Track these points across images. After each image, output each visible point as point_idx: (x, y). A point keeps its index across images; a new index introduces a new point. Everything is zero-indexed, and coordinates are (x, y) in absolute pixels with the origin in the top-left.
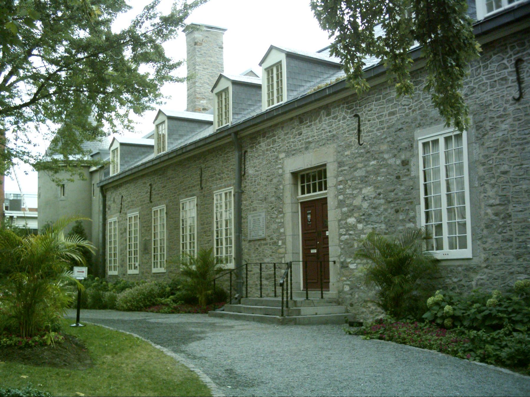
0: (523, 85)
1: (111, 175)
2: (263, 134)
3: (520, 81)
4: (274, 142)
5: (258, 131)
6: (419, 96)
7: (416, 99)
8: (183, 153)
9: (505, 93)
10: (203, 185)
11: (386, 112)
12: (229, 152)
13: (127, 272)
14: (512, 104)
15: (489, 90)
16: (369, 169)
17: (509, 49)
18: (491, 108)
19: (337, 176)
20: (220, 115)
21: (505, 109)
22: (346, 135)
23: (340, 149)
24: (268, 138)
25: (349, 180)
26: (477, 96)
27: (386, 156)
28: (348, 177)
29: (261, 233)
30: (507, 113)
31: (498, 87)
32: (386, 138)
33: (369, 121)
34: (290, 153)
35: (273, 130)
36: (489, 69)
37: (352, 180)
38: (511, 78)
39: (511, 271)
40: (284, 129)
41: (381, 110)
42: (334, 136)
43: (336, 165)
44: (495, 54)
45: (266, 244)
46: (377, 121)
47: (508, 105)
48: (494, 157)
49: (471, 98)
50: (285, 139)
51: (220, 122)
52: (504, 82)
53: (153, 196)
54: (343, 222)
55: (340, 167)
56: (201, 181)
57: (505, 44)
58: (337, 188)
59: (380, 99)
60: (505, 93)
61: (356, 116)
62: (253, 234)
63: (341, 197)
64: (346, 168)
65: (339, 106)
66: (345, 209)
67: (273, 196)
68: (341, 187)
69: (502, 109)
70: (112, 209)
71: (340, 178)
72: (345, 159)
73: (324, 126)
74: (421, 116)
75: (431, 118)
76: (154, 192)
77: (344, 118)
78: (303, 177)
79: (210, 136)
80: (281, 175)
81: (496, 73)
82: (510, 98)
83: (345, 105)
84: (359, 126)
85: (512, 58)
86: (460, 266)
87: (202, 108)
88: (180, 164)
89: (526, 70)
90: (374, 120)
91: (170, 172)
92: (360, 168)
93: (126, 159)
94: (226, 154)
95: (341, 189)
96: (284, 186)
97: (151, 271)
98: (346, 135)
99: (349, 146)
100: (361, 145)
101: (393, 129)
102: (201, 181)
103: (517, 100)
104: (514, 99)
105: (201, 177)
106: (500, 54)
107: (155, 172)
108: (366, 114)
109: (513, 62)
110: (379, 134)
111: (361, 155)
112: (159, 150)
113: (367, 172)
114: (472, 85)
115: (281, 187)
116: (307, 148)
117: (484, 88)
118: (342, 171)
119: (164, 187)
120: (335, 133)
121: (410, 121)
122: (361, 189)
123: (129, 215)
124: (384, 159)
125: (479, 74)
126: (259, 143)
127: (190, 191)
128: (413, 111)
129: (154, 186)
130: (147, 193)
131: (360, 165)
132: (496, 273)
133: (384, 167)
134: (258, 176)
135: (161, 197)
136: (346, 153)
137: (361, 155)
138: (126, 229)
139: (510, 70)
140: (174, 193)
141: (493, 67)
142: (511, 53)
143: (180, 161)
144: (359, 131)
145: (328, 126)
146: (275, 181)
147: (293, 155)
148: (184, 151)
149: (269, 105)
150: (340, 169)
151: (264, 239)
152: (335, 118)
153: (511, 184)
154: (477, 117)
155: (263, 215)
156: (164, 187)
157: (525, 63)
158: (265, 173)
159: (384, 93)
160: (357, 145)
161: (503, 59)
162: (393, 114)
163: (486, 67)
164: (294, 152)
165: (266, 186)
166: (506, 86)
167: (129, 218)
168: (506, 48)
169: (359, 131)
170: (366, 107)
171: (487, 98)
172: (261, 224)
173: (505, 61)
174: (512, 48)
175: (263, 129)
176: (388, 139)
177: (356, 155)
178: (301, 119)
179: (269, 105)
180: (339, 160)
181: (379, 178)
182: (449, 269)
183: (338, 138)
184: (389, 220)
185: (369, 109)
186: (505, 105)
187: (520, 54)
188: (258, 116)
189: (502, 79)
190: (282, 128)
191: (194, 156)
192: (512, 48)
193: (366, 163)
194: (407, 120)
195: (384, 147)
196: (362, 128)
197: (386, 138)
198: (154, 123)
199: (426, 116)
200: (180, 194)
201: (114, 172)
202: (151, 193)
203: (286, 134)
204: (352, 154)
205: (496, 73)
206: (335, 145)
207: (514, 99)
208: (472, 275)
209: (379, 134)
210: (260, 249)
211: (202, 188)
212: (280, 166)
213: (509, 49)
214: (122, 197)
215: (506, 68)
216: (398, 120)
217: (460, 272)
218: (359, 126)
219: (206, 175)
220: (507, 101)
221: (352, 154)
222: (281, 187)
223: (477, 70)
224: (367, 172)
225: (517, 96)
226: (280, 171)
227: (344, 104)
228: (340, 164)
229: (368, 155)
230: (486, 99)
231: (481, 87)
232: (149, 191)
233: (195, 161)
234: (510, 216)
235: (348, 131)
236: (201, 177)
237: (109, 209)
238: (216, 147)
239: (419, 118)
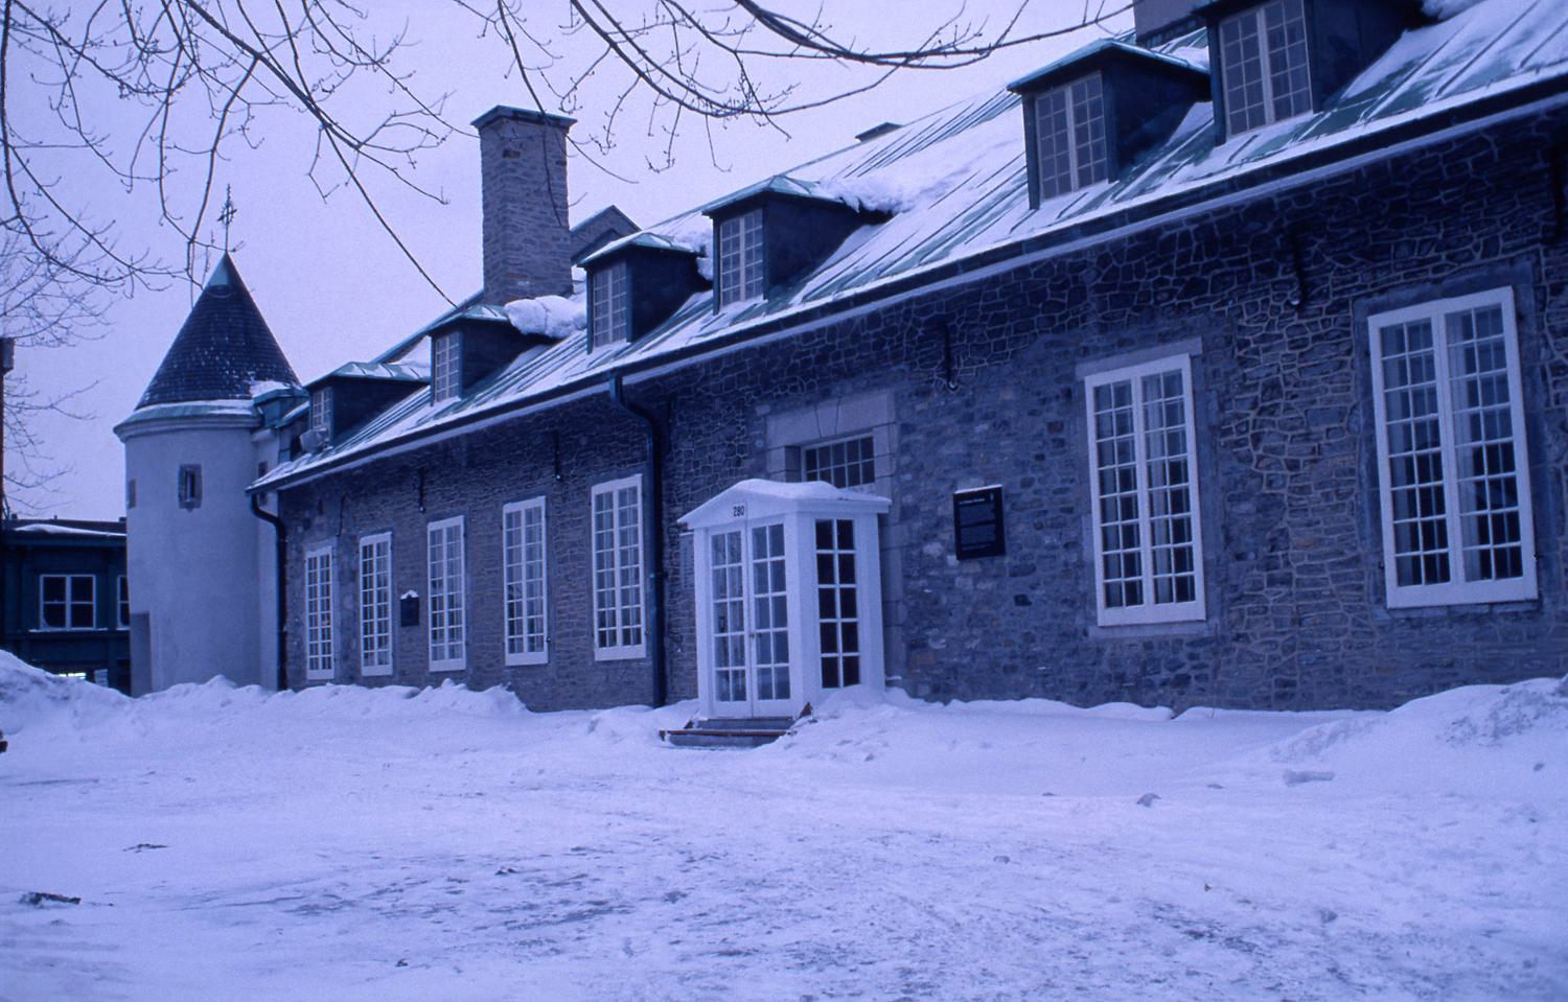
13: (359, 671)
27: (1010, 414)
43: (895, 430)
48: (1250, 419)
54: (915, 553)
63: (909, 499)
66: (918, 525)
68: (908, 477)
78: (811, 454)
95: (907, 482)
97: (427, 668)
123: (364, 541)
138: (354, 573)
167: (365, 548)
186: (1271, 318)
226: (759, 444)
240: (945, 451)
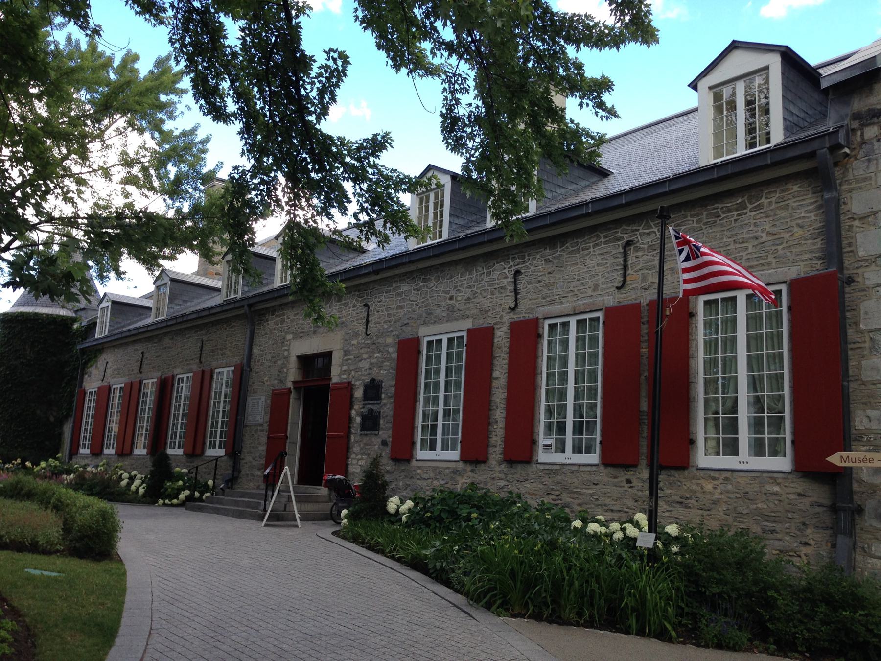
0: (518, 296)
1: (96, 337)
2: (272, 311)
3: (516, 292)
4: (283, 321)
5: (267, 308)
6: (427, 293)
7: (423, 296)
8: (183, 322)
9: (503, 301)
10: (203, 360)
11: (394, 306)
12: (235, 326)
14: (508, 313)
15: (489, 296)
16: (374, 361)
17: (510, 260)
18: (490, 314)
19: (341, 365)
20: (229, 286)
21: (501, 317)
22: (355, 323)
23: (347, 337)
24: (276, 316)
25: (353, 370)
26: (479, 301)
27: (391, 350)
28: (352, 367)
29: (258, 418)
30: (503, 321)
31: (497, 295)
32: (392, 331)
33: (378, 312)
34: (298, 336)
35: (283, 309)
36: (491, 277)
37: (356, 370)
38: (509, 288)
39: (493, 476)
40: (294, 309)
41: (390, 303)
42: (343, 323)
43: (342, 352)
44: (498, 263)
45: (263, 431)
46: (385, 313)
47: (504, 314)
49: (472, 302)
50: (294, 320)
51: (228, 293)
52: (502, 291)
53: (144, 366)
55: (345, 355)
56: (201, 354)
57: (508, 255)
58: (340, 377)
59: (390, 291)
60: (503, 301)
61: (366, 305)
62: (250, 418)
64: (351, 357)
67: (275, 379)
69: (499, 316)
70: (93, 376)
71: (345, 368)
72: (351, 348)
73: (334, 311)
74: (426, 313)
75: (436, 317)
76: (145, 361)
77: (354, 306)
79: (216, 307)
80: (286, 358)
81: (497, 281)
82: (507, 307)
83: (357, 293)
84: (368, 315)
85: (512, 269)
86: (448, 468)
87: (215, 272)
88: (179, 332)
89: (523, 282)
90: (383, 312)
91: (167, 341)
92: (365, 359)
93: (118, 320)
94: (232, 327)
96: (288, 370)
98: (355, 323)
99: (356, 335)
100: (368, 335)
101: (399, 323)
102: (201, 354)
103: (513, 309)
104: (510, 308)
105: (201, 350)
106: (502, 264)
107: (149, 339)
108: (376, 305)
109: (513, 272)
110: (386, 327)
111: (367, 346)
112: (157, 315)
113: (371, 364)
114: (475, 289)
115: (285, 370)
117: (485, 294)
118: (347, 360)
119: (158, 357)
120: (344, 319)
121: (416, 317)
124: (388, 352)
125: (482, 280)
126: (267, 321)
127: (188, 364)
128: (420, 307)
129: (146, 355)
130: (137, 362)
131: (365, 356)
132: (480, 478)
133: (388, 361)
135: (153, 367)
136: (353, 342)
137: (367, 346)
139: (509, 280)
140: (169, 365)
141: (496, 274)
142: (512, 264)
143: (180, 330)
144: (367, 322)
145: (339, 312)
146: (279, 363)
147: (301, 337)
148: (185, 319)
149: (282, 282)
150: (345, 358)
151: (262, 425)
152: (346, 304)
153: (500, 390)
154: (476, 321)
155: (263, 398)
156: (158, 357)
157: (523, 276)
158: (270, 353)
159: (394, 286)
160: (364, 335)
161: (505, 268)
162: (401, 307)
163: (489, 274)
164: (302, 335)
165: (269, 367)
166: (504, 295)
168: (509, 259)
169: (367, 322)
170: (376, 297)
171: (486, 304)
172: (260, 409)
173: (506, 271)
174: (514, 259)
175: (273, 307)
176: (394, 333)
177: (363, 345)
179: (282, 282)
180: (346, 348)
181: (382, 372)
182: (437, 471)
183: (346, 326)
184: (387, 416)
185: (379, 300)
187: (519, 266)
188: (269, 292)
189: (502, 288)
190: (293, 307)
191: (197, 326)
192: (514, 259)
193: (371, 355)
194: (413, 316)
196: (370, 319)
197: (392, 331)
198: (154, 283)
199: (431, 314)
200: (175, 367)
201: (101, 333)
202: (142, 362)
203: (295, 315)
205: (497, 281)
206: (343, 332)
207: (510, 308)
208: (458, 478)
209: (386, 327)
210: (256, 436)
211: (201, 362)
212: (286, 348)
213: (510, 260)
214: (107, 363)
215: (506, 277)
216: (405, 314)
217: (448, 475)
218: (368, 315)
219: (207, 347)
220: (503, 310)
221: (358, 343)
222: (285, 370)
223: (480, 275)
224: (371, 364)
225: (513, 306)
226: (286, 353)
227: (355, 291)
228: (346, 353)
229: (374, 347)
230: (486, 305)
231: (483, 292)
232: (140, 359)
233: (197, 332)
234: (497, 422)
235: (357, 320)
236: (201, 350)
237: (89, 376)
238: (221, 319)
239: (424, 315)
240: (361, 365)
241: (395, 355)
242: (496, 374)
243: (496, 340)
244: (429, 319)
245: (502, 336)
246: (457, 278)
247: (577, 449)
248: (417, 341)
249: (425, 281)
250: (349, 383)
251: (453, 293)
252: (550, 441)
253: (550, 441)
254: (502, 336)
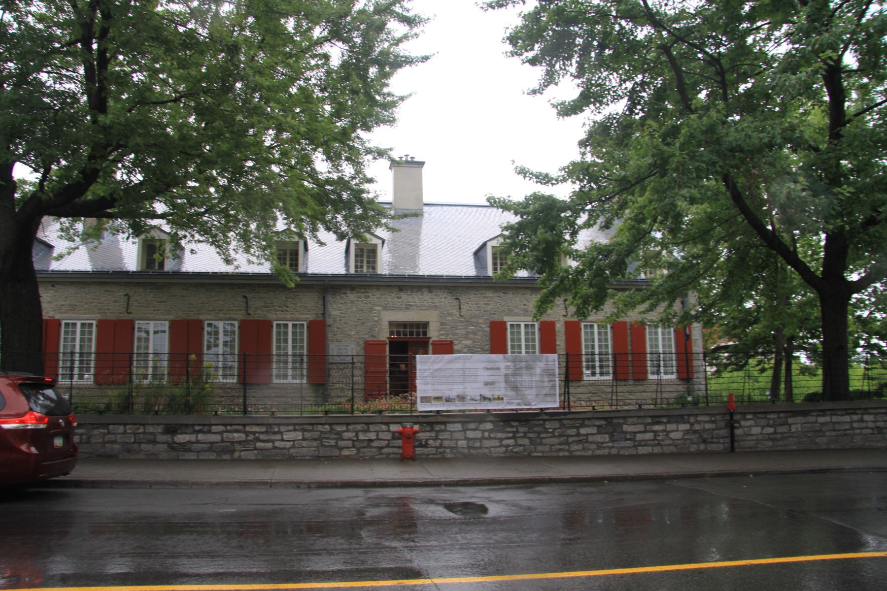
19: (440, 330)
23: (442, 315)
27: (482, 326)
37: (453, 335)
43: (438, 324)
65: (441, 289)
71: (443, 332)
77: (445, 298)
111: (461, 322)
116: (407, 309)
122: (461, 341)
131: (460, 327)
134: (344, 317)
137: (461, 322)
144: (460, 308)
162: (488, 304)
169: (460, 308)
178: (401, 289)
195: (480, 321)
203: (382, 295)
204: (453, 319)
221: (453, 319)
226: (376, 319)
241: (488, 329)
242: (558, 343)
243: (557, 328)
244: (510, 313)
245: (560, 327)
246: (528, 296)
247: (602, 374)
248: (504, 324)
249: (505, 293)
250: (452, 342)
251: (525, 302)
252: (589, 372)
253: (589, 372)
254: (560, 327)
